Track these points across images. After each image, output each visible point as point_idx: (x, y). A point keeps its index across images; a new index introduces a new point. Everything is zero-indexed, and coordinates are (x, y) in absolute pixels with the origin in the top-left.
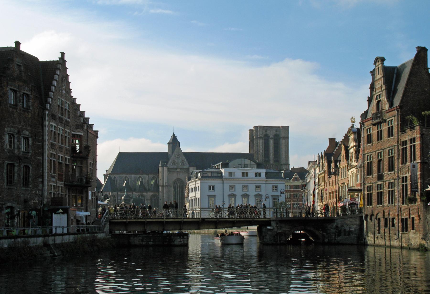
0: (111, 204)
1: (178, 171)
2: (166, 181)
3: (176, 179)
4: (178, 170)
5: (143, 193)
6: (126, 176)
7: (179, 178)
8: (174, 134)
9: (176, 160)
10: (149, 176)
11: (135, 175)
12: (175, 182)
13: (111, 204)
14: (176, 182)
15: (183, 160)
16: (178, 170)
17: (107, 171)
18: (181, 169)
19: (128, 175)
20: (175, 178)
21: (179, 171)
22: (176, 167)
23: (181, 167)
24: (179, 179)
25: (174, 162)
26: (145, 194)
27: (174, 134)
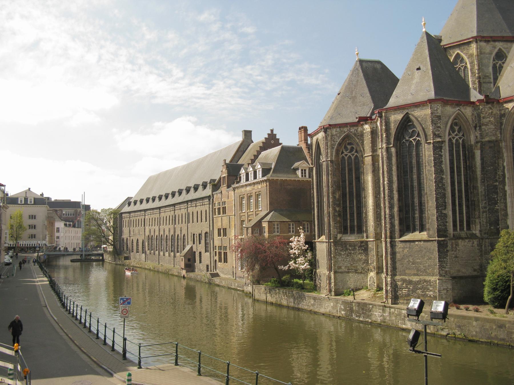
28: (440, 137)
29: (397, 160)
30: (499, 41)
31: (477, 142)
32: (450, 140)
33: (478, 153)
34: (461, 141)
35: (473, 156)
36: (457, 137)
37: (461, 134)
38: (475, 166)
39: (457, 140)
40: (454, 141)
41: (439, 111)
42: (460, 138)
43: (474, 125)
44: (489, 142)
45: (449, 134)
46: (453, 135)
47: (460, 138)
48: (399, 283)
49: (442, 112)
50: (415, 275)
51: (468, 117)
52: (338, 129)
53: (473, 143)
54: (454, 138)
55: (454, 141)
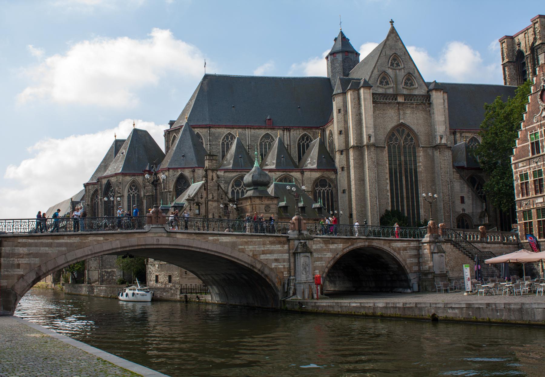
0: (210, 197)
1: (399, 103)
2: (371, 132)
3: (394, 128)
4: (400, 99)
5: (291, 174)
6: (230, 134)
7: (402, 125)
8: (342, 33)
9: (390, 72)
10: (292, 132)
11: (253, 131)
12: (391, 135)
13: (210, 197)
14: (393, 135)
15: (409, 73)
16: (400, 99)
17: (172, 123)
18: (406, 97)
19: (235, 130)
20: (391, 125)
21: (403, 104)
22: (390, 91)
23: (405, 92)
24: (401, 128)
25: (384, 78)
26: (296, 175)
27: (342, 33)
28: (120, 194)
29: (105, 206)
30: (197, 128)
31: (144, 196)
32: (129, 195)
33: (145, 201)
34: (136, 195)
35: (142, 203)
36: (133, 193)
37: (136, 192)
38: (143, 209)
39: (134, 194)
40: (131, 195)
41: (120, 179)
42: (136, 193)
43: (144, 186)
44: (149, 196)
45: (129, 191)
46: (131, 192)
47: (136, 193)
48: (104, 273)
49: (122, 180)
50: (110, 268)
51: (140, 182)
52: (92, 186)
53: (142, 196)
54: (131, 193)
55: (131, 195)
